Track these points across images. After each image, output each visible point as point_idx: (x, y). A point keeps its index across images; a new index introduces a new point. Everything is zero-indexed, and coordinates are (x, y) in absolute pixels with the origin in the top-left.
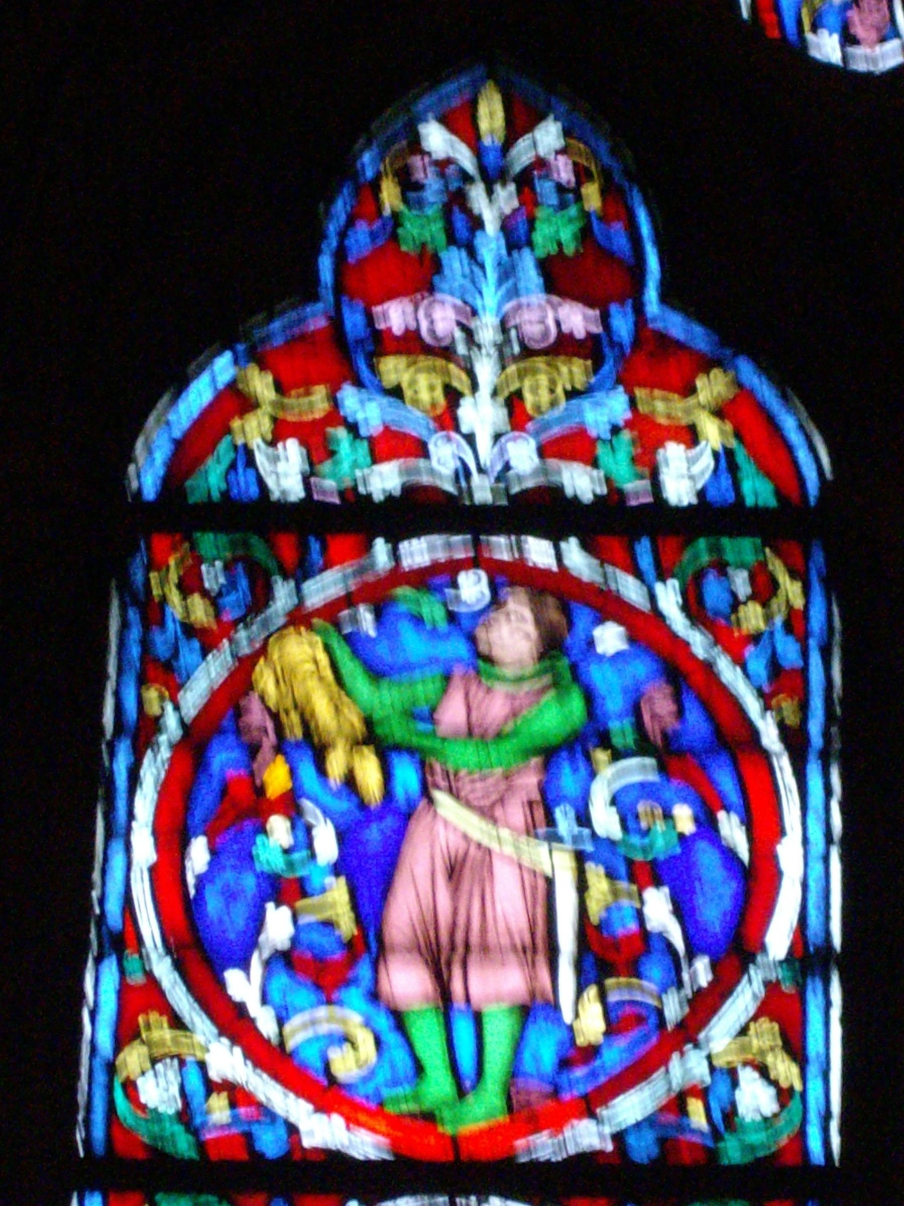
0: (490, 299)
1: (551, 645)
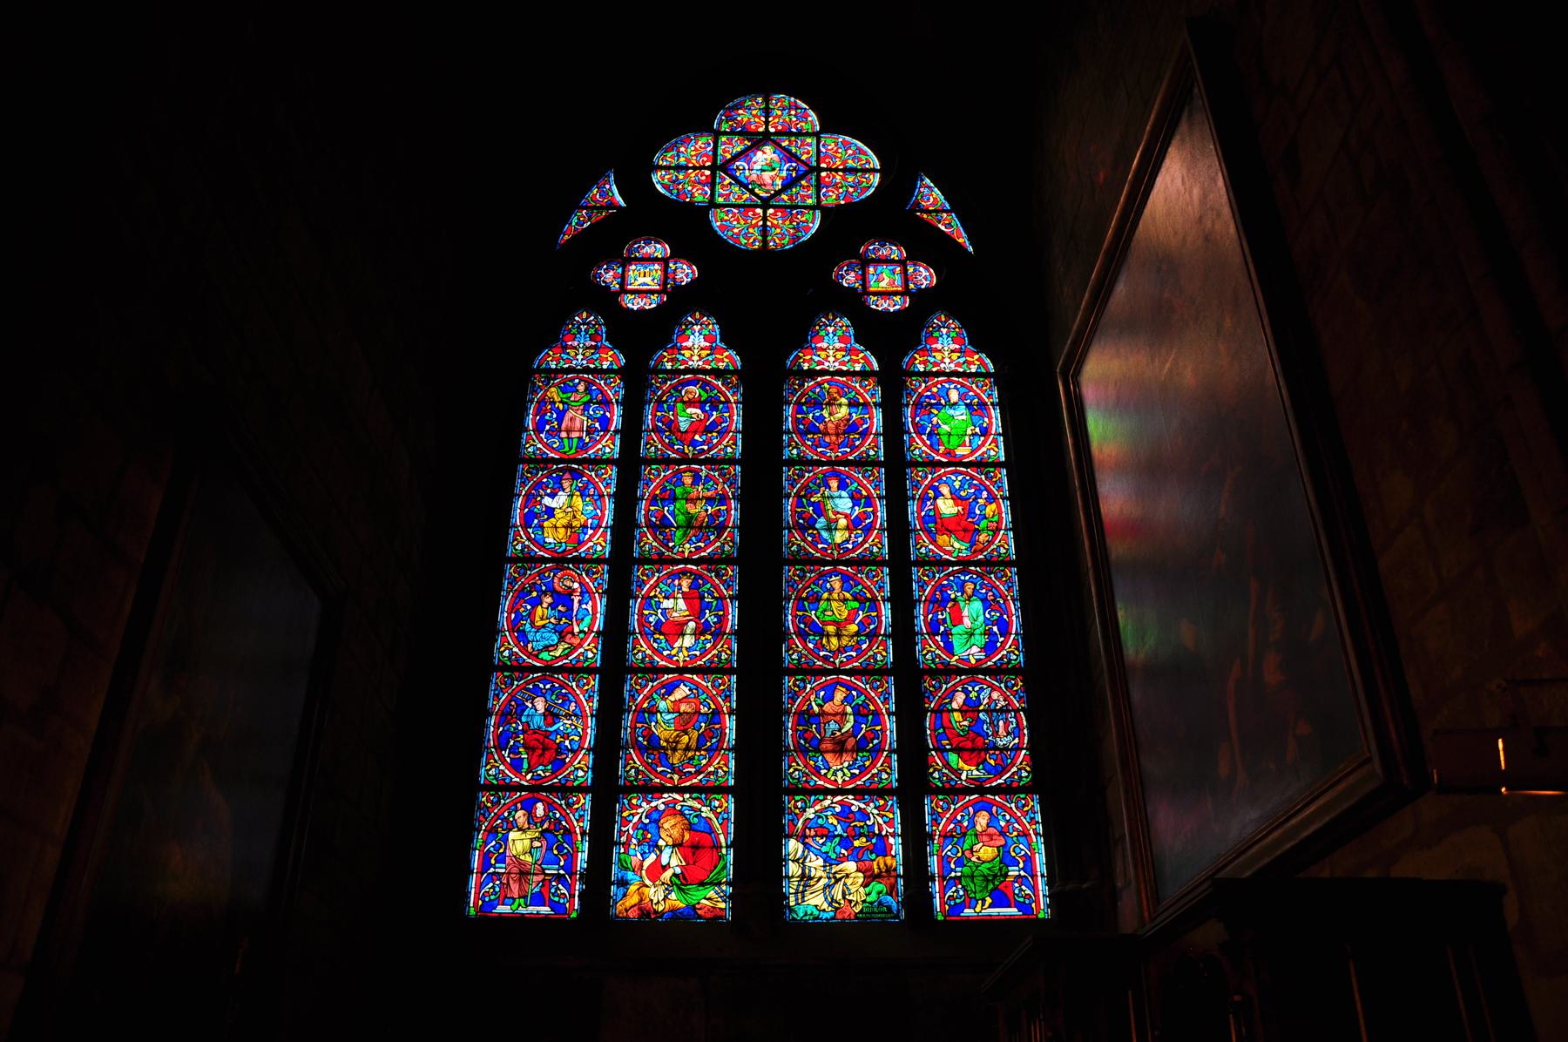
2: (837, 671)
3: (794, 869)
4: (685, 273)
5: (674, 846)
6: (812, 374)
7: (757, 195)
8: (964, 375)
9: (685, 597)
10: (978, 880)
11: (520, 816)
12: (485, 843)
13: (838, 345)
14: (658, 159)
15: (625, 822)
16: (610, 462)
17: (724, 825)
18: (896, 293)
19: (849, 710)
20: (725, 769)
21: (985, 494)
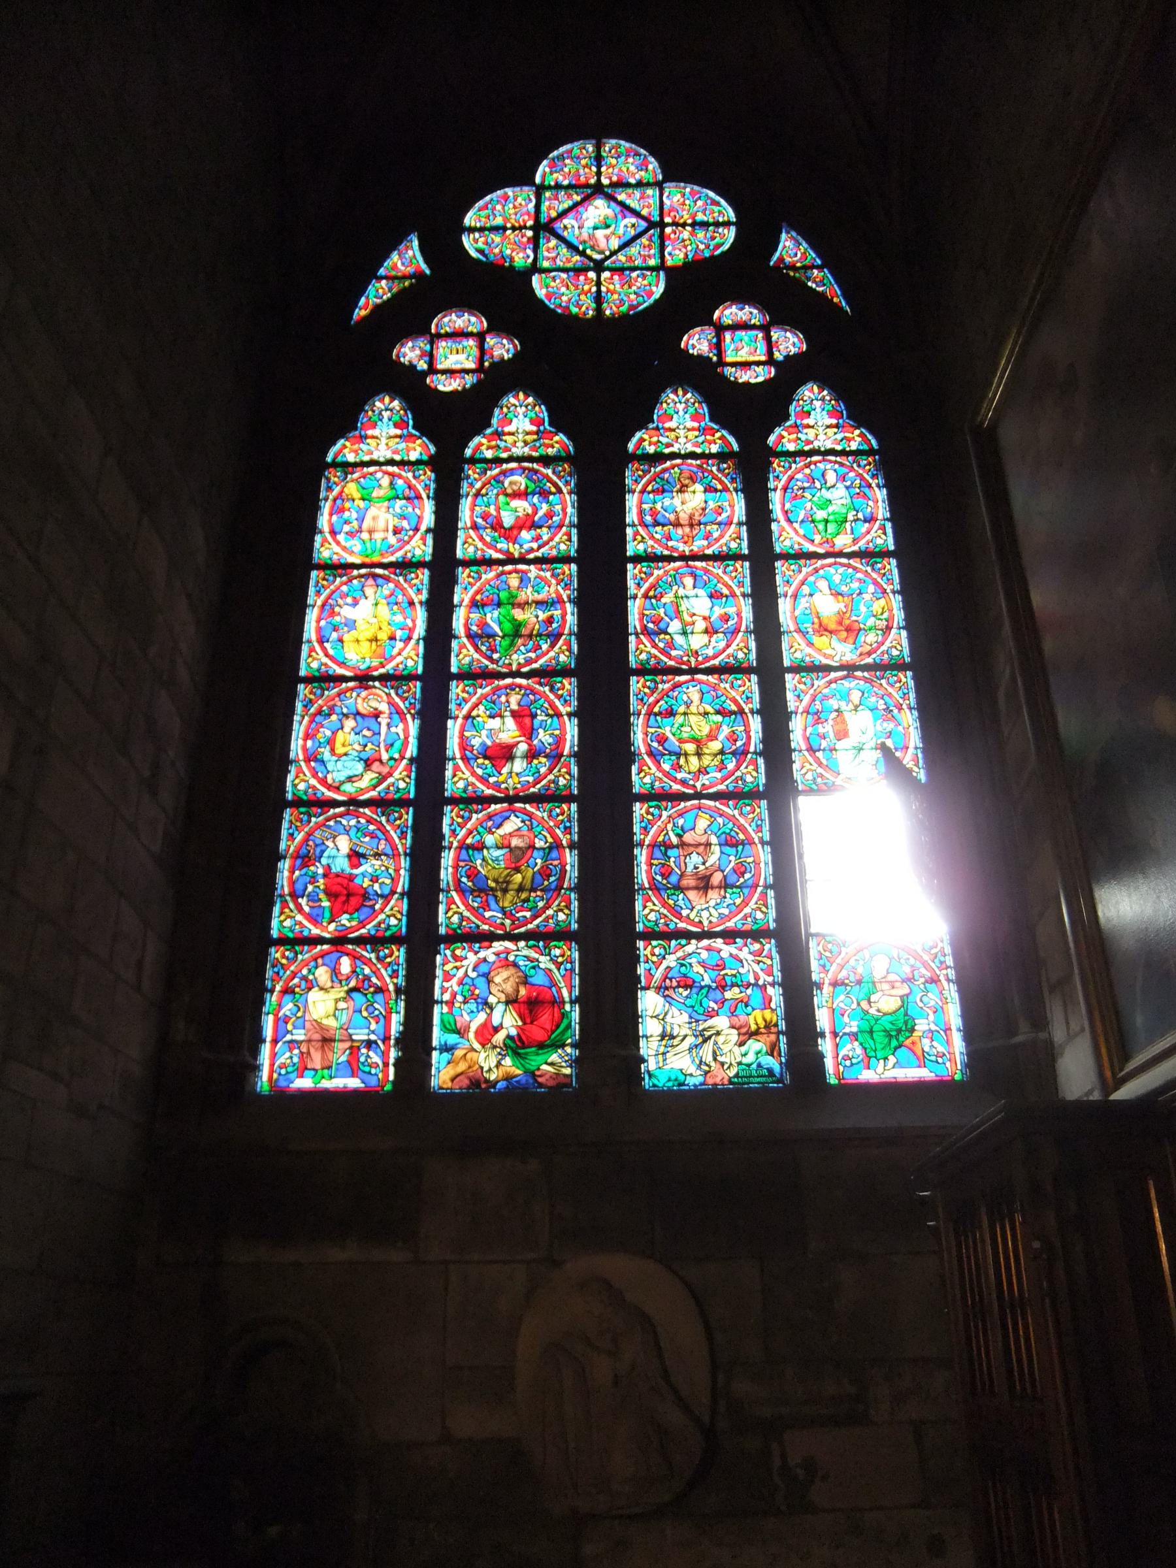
0: (385, 430)
1: (391, 483)
2: (698, 796)
3: (649, 1027)
4: (503, 348)
5: (507, 1003)
6: (659, 458)
7: (590, 258)
8: (843, 453)
9: (514, 714)
10: (879, 1037)
11: (322, 974)
12: (280, 1006)
13: (691, 424)
14: (470, 219)
15: (448, 977)
16: (421, 564)
17: (568, 977)
18: (758, 363)
19: (714, 840)
20: (564, 914)
21: (871, 588)
